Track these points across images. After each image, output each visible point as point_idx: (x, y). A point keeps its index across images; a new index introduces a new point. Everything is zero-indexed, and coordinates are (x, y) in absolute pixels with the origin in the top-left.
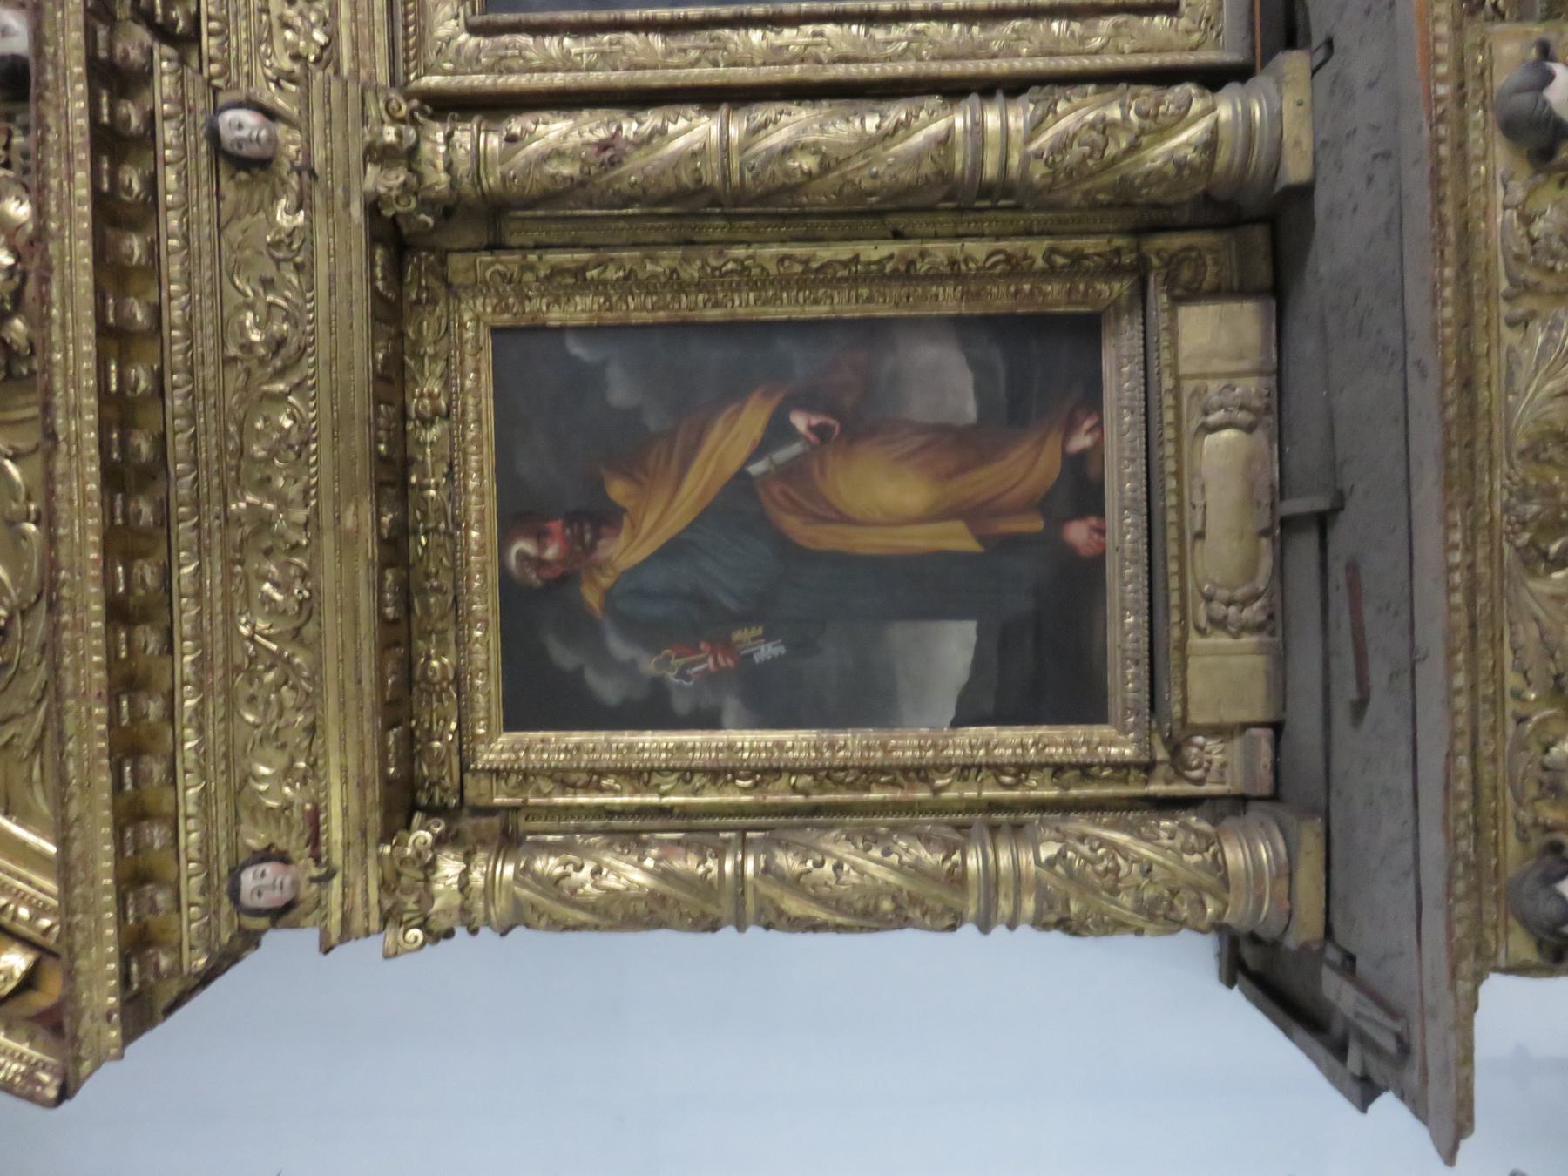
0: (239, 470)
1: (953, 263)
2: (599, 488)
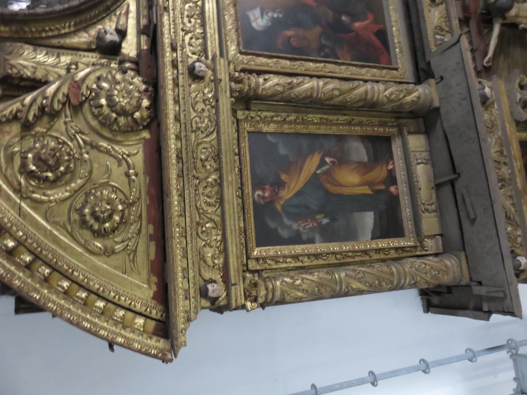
2: (278, 176)
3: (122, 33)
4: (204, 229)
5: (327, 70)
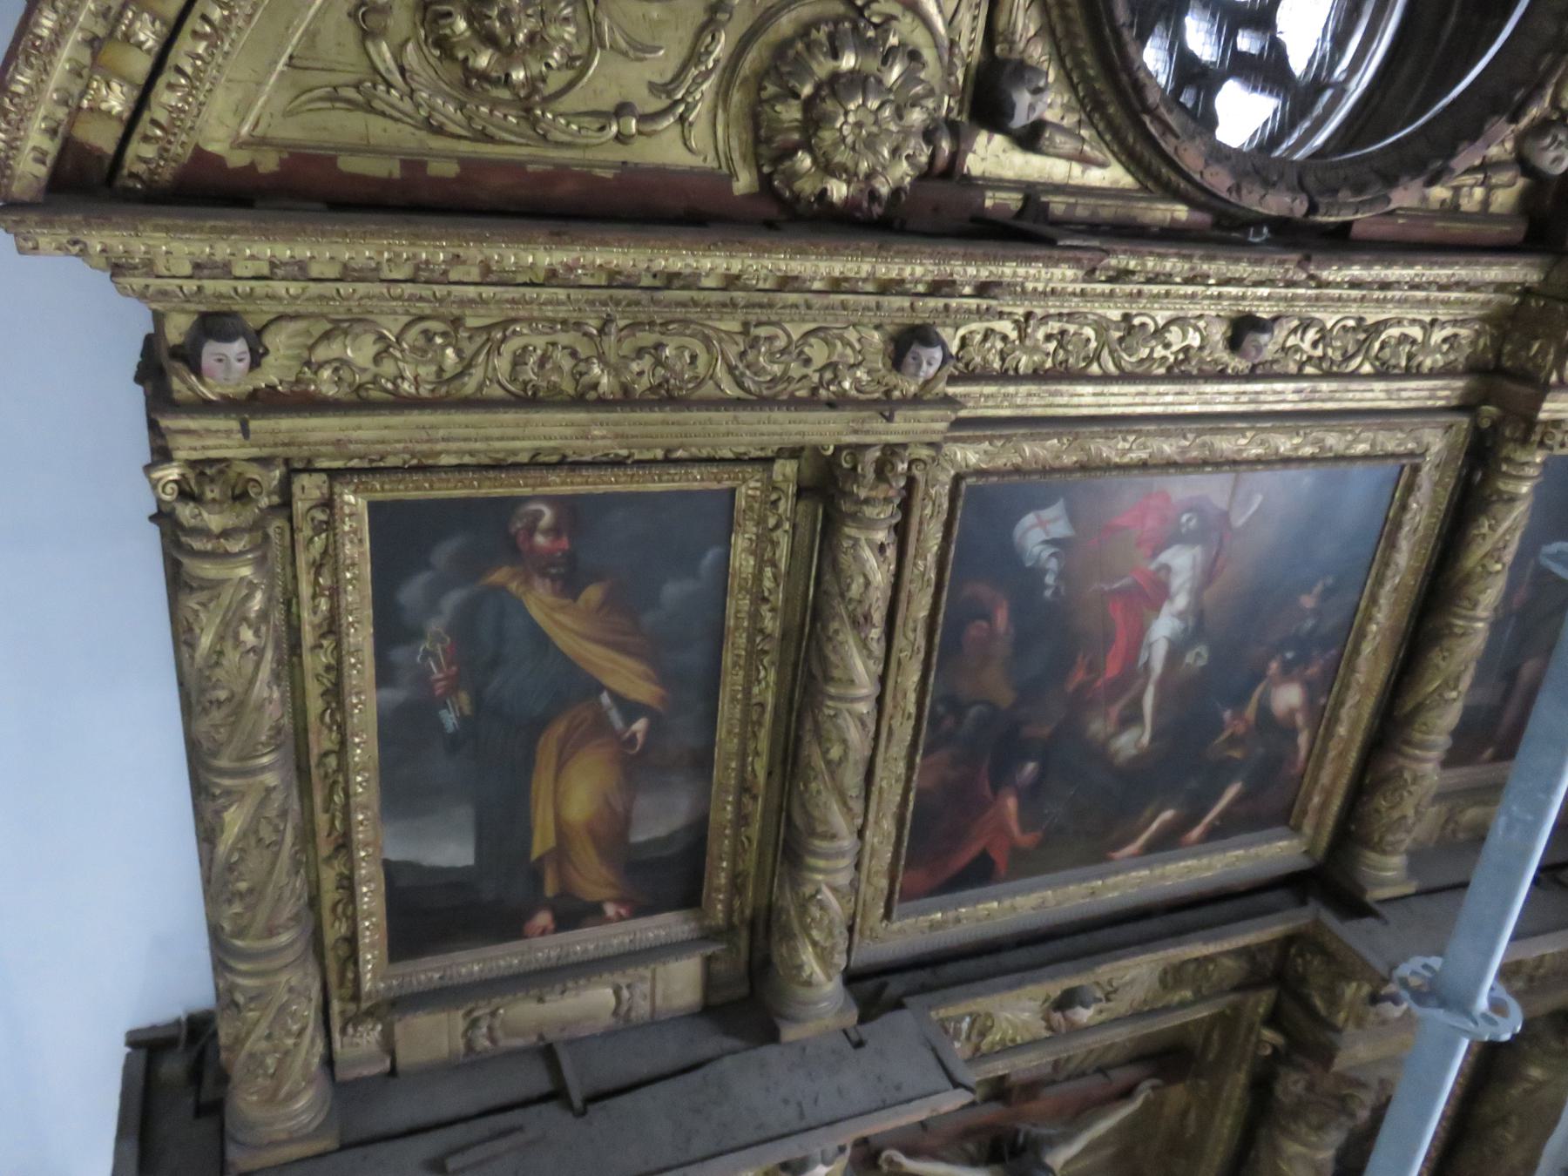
2: (595, 577)
3: (1030, 139)
4: (439, 340)
5: (896, 723)
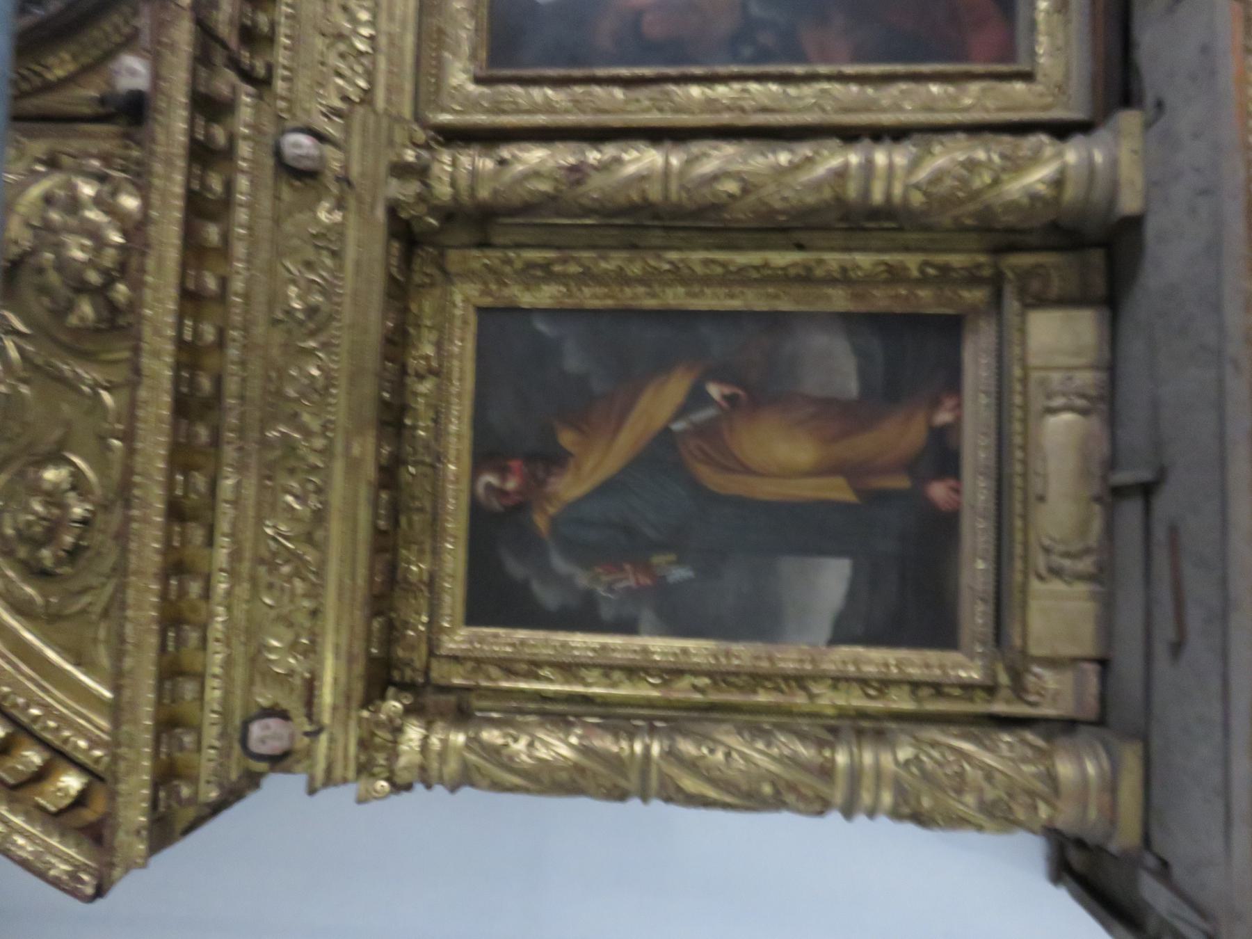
0: (276, 405)
1: (844, 270)
